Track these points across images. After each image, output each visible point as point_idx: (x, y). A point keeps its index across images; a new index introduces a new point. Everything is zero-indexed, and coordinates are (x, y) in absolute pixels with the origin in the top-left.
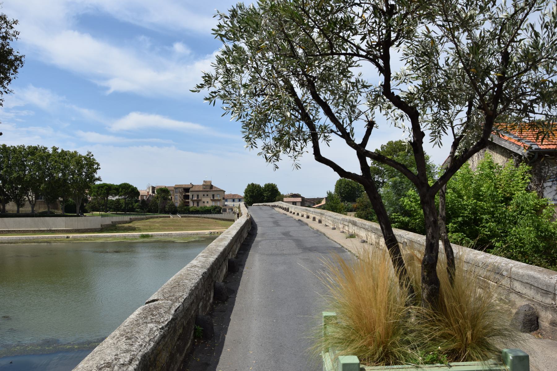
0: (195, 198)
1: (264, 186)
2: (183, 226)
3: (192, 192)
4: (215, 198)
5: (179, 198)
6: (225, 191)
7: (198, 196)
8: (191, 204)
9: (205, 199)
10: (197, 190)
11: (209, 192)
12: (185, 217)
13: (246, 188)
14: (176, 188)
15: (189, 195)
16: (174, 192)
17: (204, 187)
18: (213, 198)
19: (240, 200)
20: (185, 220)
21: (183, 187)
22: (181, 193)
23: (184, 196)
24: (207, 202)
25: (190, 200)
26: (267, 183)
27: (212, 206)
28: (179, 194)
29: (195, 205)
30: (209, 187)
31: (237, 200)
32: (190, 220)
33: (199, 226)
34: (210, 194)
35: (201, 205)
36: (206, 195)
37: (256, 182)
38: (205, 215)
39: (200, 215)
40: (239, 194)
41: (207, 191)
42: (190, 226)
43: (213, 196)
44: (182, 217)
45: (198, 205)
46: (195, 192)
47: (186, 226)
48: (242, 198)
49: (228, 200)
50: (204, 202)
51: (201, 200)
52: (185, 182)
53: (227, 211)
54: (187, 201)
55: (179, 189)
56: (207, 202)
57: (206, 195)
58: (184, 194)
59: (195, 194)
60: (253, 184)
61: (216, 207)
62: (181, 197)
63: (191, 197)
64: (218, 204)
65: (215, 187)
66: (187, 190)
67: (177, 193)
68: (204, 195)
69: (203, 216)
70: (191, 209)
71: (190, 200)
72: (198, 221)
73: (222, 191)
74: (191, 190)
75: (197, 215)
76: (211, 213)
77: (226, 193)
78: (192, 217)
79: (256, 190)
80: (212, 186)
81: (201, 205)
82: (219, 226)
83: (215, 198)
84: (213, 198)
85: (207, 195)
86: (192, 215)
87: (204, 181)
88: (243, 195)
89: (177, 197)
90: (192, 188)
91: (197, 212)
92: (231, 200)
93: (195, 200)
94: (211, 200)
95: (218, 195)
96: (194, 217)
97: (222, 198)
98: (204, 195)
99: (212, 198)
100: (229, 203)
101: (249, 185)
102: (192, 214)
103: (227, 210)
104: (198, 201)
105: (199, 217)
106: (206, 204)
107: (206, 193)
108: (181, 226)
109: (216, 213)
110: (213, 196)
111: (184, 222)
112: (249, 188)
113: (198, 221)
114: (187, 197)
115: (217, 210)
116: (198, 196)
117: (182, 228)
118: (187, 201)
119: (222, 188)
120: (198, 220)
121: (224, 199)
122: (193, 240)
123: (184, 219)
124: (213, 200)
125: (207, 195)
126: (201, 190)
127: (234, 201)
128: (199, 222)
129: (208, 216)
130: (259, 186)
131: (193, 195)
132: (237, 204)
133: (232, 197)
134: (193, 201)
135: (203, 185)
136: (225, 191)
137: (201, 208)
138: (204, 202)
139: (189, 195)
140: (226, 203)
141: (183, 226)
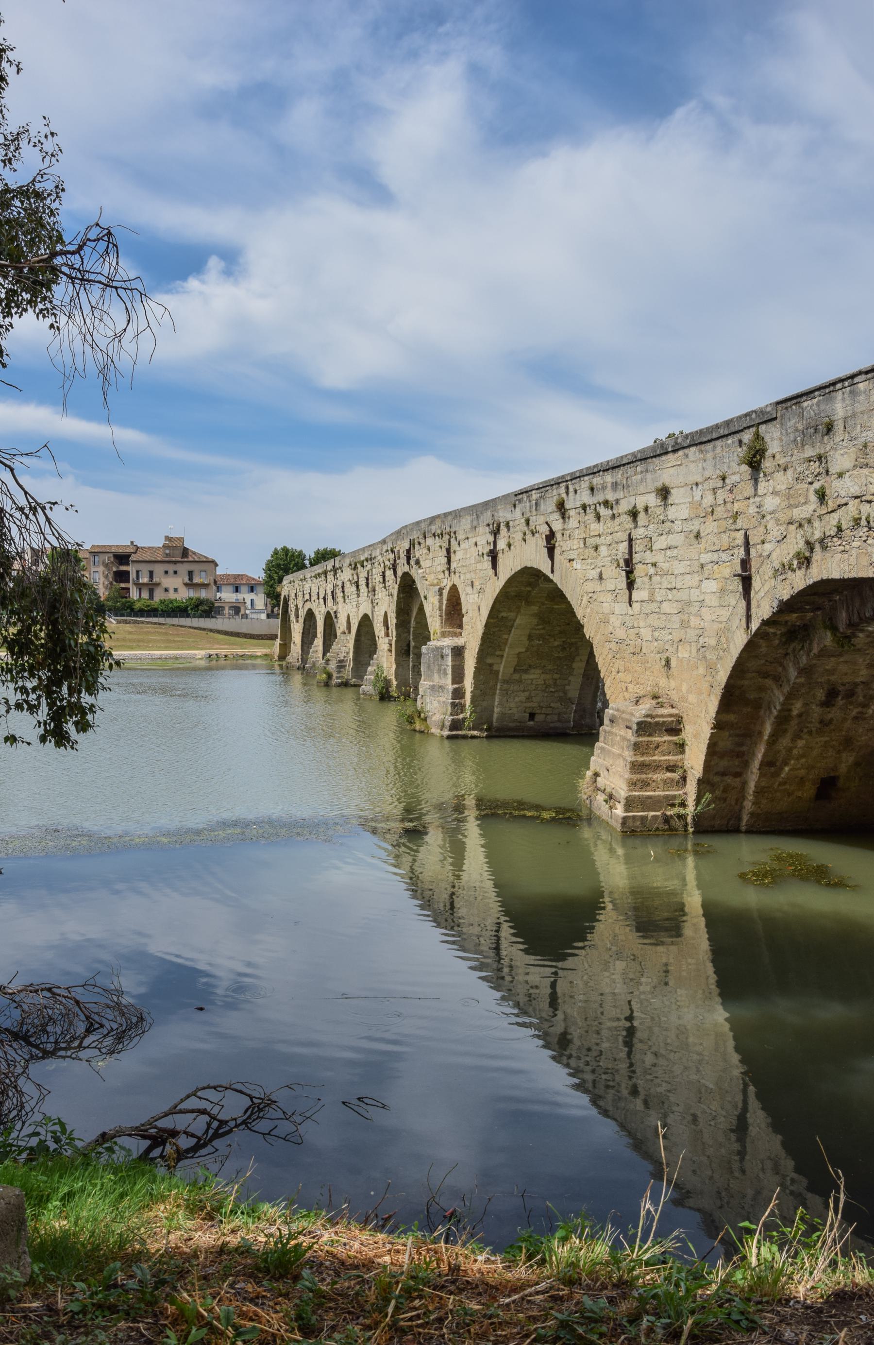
0: (144, 579)
1: (313, 556)
2: (130, 641)
3: (136, 565)
4: (196, 580)
5: (102, 579)
6: (216, 565)
7: (151, 573)
8: (134, 594)
9: (170, 582)
10: (149, 559)
11: (179, 565)
12: (126, 622)
13: (270, 558)
14: (95, 553)
15: (128, 572)
16: (88, 563)
17: (167, 551)
18: (191, 579)
19: (252, 589)
20: (130, 630)
21: (113, 550)
22: (106, 565)
23: (115, 573)
24: (176, 590)
25: (130, 585)
26: (322, 548)
27: (191, 599)
28: (101, 569)
29: (145, 595)
30: (179, 552)
31: (244, 589)
32: (142, 628)
33: (169, 641)
34: (183, 569)
35: (159, 595)
36: (171, 572)
37: (294, 545)
38: (175, 621)
39: (161, 620)
40: (250, 575)
41: (175, 562)
42: (149, 641)
43: (190, 574)
44: (118, 622)
45: (151, 596)
46: (143, 565)
47: (139, 641)
48: (259, 584)
49: (224, 588)
50: (166, 590)
51: (158, 584)
52: (119, 540)
53: (226, 611)
54: (123, 585)
55: (101, 555)
56: (176, 590)
57: (171, 572)
58: (114, 569)
59: (145, 569)
60: (286, 550)
61: (200, 603)
62: (106, 577)
63: (133, 576)
64: (203, 594)
65: (195, 553)
66: (122, 558)
67: (98, 566)
68: (166, 572)
69: (169, 621)
70: (137, 606)
71: (130, 585)
72: (163, 631)
73: (213, 562)
74: (133, 558)
75: (155, 620)
76: (188, 616)
77: (220, 571)
78: (143, 622)
79: (294, 566)
80: (185, 552)
81: (159, 595)
82: (218, 643)
83: (196, 580)
84: (191, 579)
85: (175, 572)
86: (143, 619)
87: (167, 538)
88: (258, 574)
89: (97, 576)
90: (135, 553)
91: (152, 612)
92: (231, 588)
93: (144, 584)
94: (186, 585)
95: (203, 574)
96: (148, 623)
97: (212, 581)
98: (166, 572)
99: (187, 580)
100: (227, 596)
101: (276, 552)
102: (142, 616)
103: (227, 609)
104: (152, 587)
105: (160, 624)
106: (172, 595)
107: (171, 568)
108: (124, 640)
109: (201, 616)
110: (190, 574)
111: (130, 633)
112: (277, 559)
113: (163, 631)
114: (121, 576)
115: (208, 609)
116: (151, 573)
117: (128, 644)
118: (123, 585)
119: (211, 556)
120: (162, 629)
121: (215, 582)
122: (181, 666)
123: (128, 627)
124: (190, 585)
125: (175, 572)
126: (160, 558)
127: (237, 590)
128: (166, 634)
129: (183, 621)
130: (301, 555)
131: (138, 572)
132: (248, 597)
133: (232, 581)
134: (140, 586)
135: (165, 546)
136: (216, 565)
137: (162, 602)
138: (166, 590)
139: (128, 572)
140: (219, 595)
141: (130, 641)
